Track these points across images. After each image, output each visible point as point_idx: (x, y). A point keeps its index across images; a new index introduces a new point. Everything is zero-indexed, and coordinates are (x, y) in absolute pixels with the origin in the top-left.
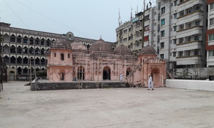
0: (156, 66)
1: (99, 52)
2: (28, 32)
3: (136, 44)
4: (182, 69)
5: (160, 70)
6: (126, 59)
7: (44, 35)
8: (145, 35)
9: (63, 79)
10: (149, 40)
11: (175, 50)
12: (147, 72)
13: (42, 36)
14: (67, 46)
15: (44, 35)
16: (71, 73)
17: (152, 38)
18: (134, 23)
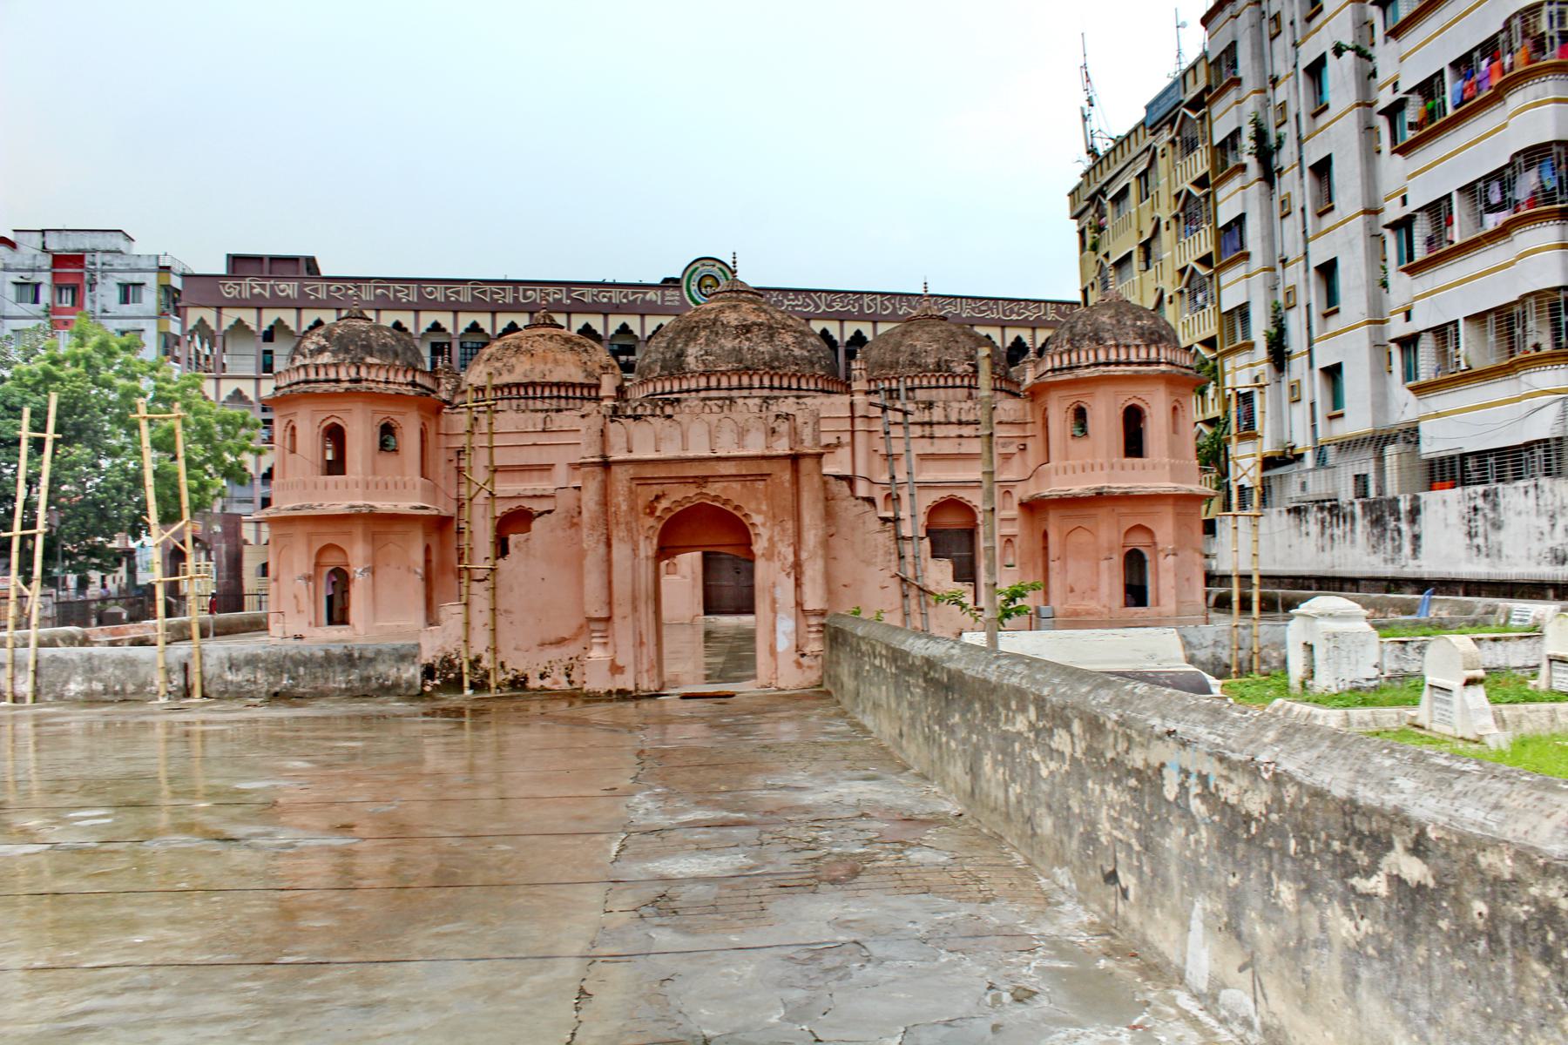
0: (705, 479)
1: (685, 387)
2: (414, 298)
3: (1181, 292)
4: (1458, 490)
5: (757, 519)
6: (923, 424)
7: (516, 298)
8: (1225, 216)
9: (337, 613)
10: (1247, 256)
11: (1408, 317)
12: (609, 545)
13: (507, 309)
14: (369, 366)
15: (516, 298)
16: (409, 569)
17: (1270, 237)
18: (1155, 128)
